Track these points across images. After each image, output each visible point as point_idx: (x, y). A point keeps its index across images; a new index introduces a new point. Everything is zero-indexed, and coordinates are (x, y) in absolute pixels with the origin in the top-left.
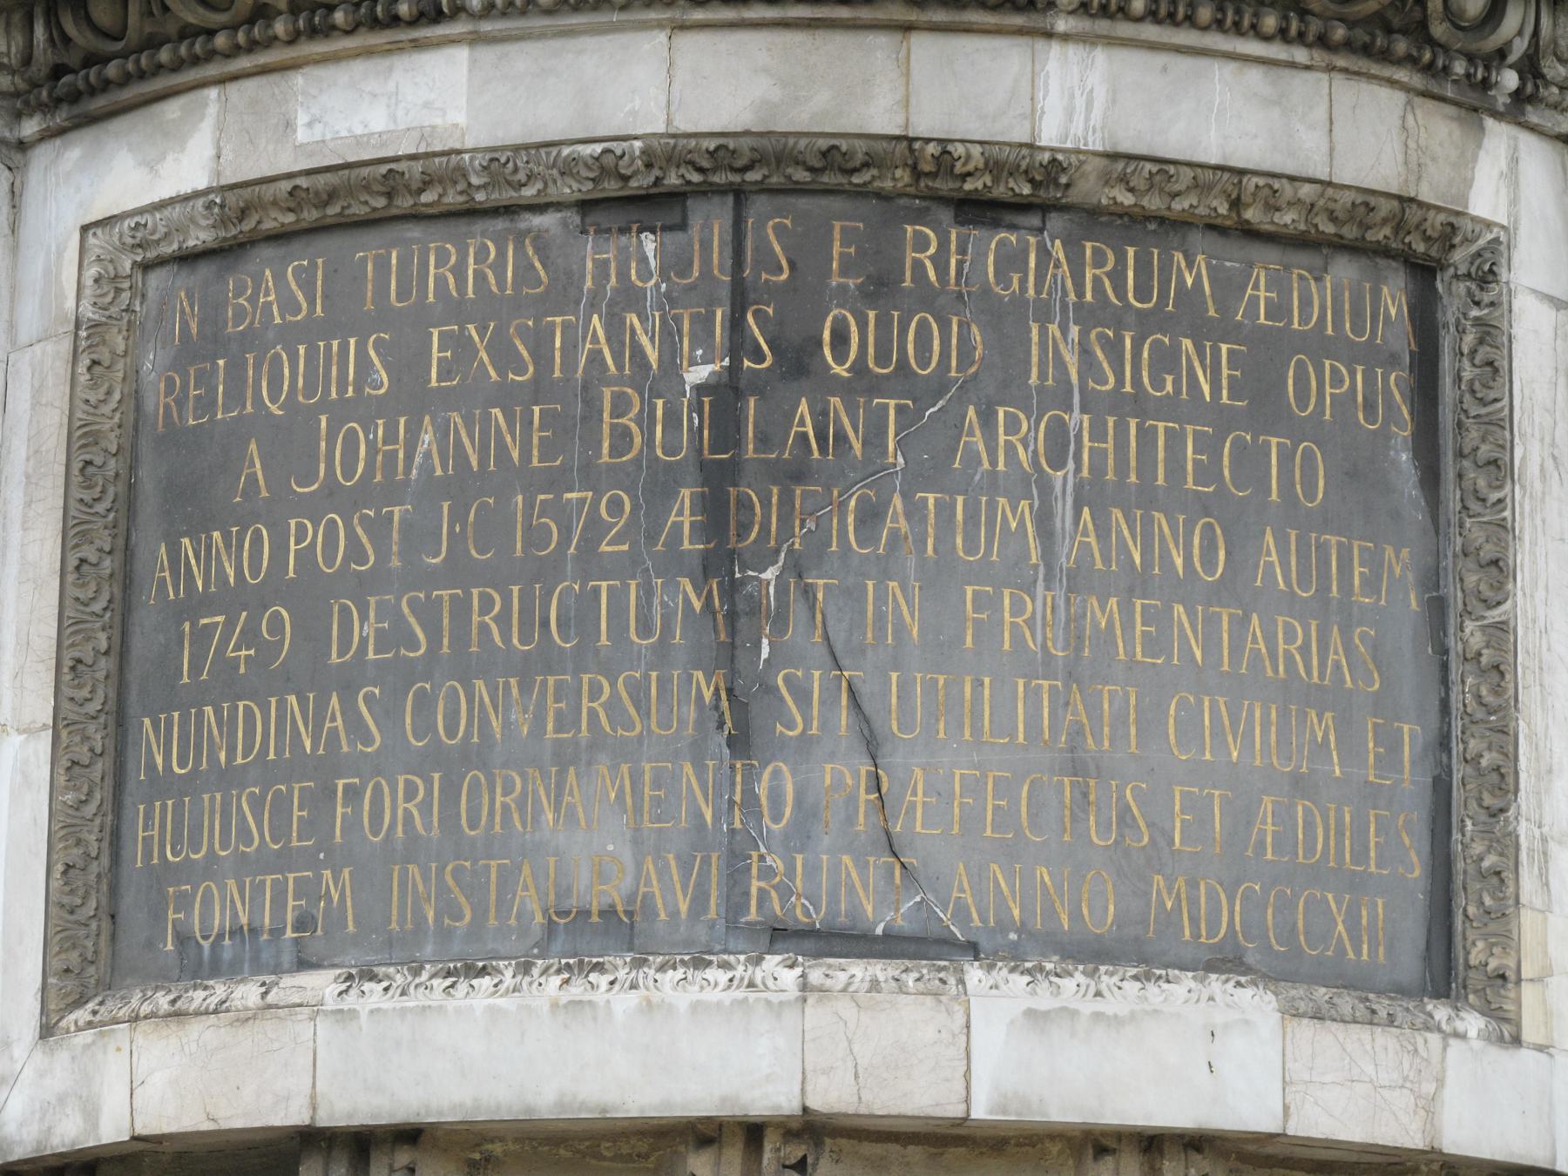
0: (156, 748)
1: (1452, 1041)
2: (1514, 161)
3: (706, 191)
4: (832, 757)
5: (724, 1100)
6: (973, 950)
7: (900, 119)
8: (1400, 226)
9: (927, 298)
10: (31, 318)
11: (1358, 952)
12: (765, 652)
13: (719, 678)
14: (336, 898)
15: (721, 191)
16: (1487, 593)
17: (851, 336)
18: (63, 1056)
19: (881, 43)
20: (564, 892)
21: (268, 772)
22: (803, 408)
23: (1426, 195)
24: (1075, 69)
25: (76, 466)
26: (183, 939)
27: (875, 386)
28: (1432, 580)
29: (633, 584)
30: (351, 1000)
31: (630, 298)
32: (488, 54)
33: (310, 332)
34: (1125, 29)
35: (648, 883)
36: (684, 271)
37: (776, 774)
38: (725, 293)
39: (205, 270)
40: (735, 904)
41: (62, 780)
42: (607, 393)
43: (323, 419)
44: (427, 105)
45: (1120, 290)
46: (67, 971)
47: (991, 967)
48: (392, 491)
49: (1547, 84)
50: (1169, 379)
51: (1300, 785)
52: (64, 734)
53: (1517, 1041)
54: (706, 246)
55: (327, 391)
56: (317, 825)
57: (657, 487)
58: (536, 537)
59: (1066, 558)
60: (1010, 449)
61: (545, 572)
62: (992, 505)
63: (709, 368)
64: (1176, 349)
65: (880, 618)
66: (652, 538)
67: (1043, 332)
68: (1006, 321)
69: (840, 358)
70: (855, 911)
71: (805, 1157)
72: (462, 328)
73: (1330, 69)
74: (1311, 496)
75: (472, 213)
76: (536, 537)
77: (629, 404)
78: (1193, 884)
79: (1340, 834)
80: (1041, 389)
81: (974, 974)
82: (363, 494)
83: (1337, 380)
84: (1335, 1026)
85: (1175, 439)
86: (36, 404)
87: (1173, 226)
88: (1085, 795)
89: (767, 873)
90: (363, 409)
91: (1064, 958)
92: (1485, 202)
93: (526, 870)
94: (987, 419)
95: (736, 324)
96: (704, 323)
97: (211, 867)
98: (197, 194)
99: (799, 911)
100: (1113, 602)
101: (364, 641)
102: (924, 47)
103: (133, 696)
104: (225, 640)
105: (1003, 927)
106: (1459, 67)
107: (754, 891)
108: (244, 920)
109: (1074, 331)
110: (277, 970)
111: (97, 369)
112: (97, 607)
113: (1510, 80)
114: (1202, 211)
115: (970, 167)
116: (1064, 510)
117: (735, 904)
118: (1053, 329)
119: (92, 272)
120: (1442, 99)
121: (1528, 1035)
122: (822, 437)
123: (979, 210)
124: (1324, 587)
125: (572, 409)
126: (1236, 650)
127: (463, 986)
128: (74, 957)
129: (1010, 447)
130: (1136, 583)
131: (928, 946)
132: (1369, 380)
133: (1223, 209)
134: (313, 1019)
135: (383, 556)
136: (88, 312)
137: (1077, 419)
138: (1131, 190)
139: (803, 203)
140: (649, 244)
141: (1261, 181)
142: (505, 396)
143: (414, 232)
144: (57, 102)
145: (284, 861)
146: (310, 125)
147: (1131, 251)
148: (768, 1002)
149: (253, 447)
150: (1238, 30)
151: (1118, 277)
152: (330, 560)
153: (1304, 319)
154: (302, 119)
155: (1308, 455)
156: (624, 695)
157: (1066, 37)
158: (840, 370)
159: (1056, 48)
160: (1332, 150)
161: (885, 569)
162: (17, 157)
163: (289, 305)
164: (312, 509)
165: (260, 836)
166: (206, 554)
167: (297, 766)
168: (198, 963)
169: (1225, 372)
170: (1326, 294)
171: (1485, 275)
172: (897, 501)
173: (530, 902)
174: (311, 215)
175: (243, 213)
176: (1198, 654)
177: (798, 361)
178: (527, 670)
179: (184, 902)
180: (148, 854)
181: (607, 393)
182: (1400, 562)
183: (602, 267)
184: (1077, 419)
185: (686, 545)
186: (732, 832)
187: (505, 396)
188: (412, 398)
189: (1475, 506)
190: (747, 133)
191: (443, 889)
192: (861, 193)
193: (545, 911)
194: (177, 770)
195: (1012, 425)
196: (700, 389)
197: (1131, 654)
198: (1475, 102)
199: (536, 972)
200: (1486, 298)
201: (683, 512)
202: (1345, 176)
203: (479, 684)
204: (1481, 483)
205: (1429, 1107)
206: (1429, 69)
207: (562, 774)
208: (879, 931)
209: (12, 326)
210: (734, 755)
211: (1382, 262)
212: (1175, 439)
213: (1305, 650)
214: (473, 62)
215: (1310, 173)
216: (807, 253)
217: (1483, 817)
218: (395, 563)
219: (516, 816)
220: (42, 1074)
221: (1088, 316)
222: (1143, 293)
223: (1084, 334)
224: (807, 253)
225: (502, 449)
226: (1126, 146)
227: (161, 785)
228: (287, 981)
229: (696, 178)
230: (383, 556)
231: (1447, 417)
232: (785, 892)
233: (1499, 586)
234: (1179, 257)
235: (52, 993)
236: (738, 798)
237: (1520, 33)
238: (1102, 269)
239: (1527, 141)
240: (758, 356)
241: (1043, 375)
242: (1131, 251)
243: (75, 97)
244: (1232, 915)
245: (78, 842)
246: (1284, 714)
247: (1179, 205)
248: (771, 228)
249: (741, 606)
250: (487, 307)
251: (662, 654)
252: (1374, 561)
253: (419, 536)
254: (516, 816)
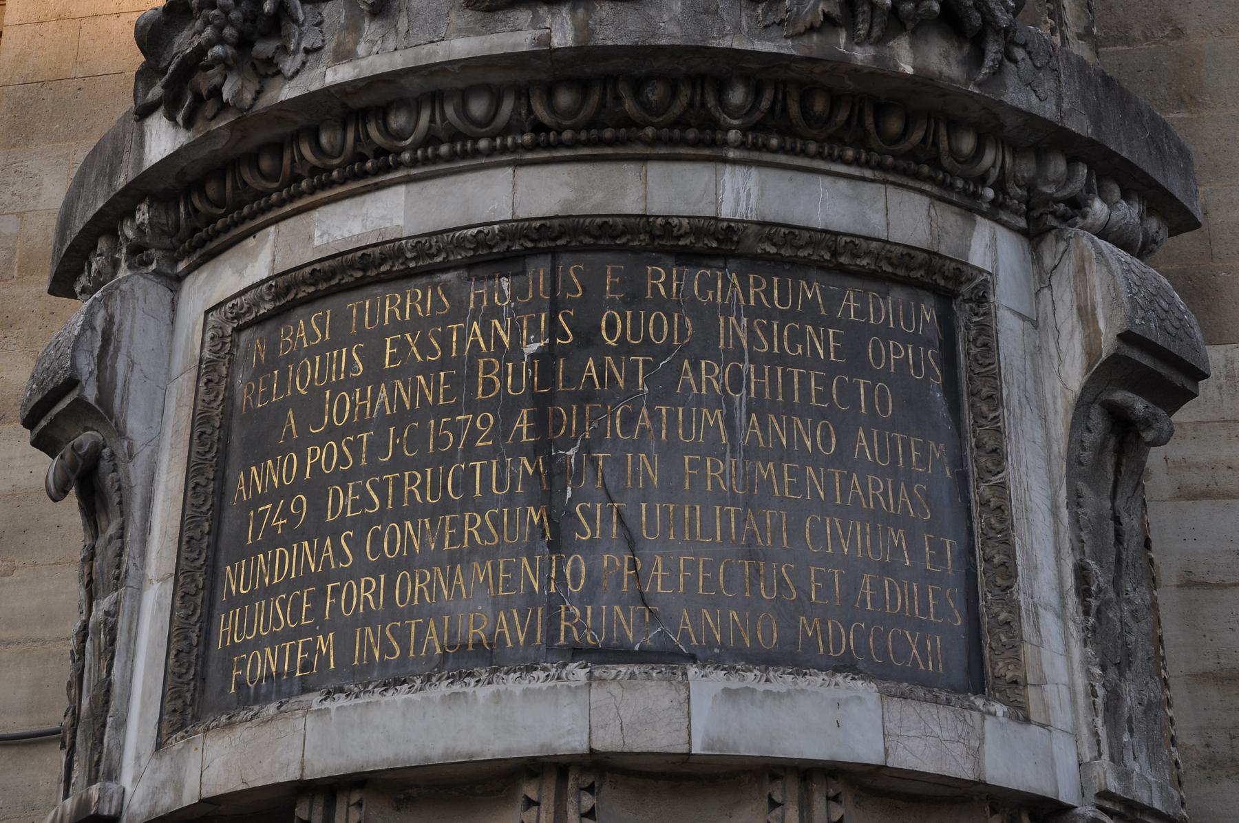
0: (234, 582)
1: (987, 717)
2: (994, 239)
3: (535, 252)
4: (608, 551)
5: (542, 746)
6: (693, 658)
7: (642, 206)
8: (930, 270)
9: (659, 303)
10: (178, 362)
11: (927, 666)
12: (569, 495)
13: (542, 510)
14: (324, 650)
15: (544, 252)
16: (992, 467)
17: (615, 326)
18: (167, 758)
19: (630, 169)
20: (453, 635)
21: (289, 585)
22: (591, 363)
23: (943, 251)
24: (740, 179)
25: (196, 435)
26: (241, 684)
27: (632, 350)
28: (958, 461)
29: (494, 462)
30: (327, 704)
31: (495, 312)
32: (415, 188)
33: (324, 348)
34: (768, 157)
35: (501, 626)
36: (524, 296)
37: (576, 561)
38: (546, 306)
39: (269, 326)
40: (551, 635)
41: (178, 603)
42: (481, 362)
43: (328, 393)
44: (383, 218)
45: (770, 299)
46: (175, 711)
47: (704, 667)
48: (363, 426)
49: (1011, 199)
50: (800, 347)
51: (885, 569)
52: (181, 578)
53: (1027, 720)
54: (536, 282)
55: (330, 378)
56: (314, 612)
57: (508, 409)
58: (441, 441)
59: (743, 440)
60: (709, 382)
61: (446, 460)
62: (699, 413)
63: (538, 345)
64: (803, 332)
65: (635, 474)
66: (505, 437)
67: (727, 322)
68: (705, 316)
69: (611, 337)
70: (623, 636)
71: (593, 783)
72: (403, 336)
73: (885, 182)
74: (885, 411)
75: (408, 275)
76: (441, 441)
77: (493, 367)
78: (824, 623)
79: (911, 598)
80: (726, 351)
81: (693, 670)
82: (350, 428)
83: (897, 352)
84: (913, 703)
85: (804, 379)
86: (178, 406)
87: (800, 266)
88: (758, 571)
89: (570, 617)
90: (350, 385)
91: (749, 661)
92: (978, 256)
93: (432, 625)
94: (695, 367)
95: (552, 321)
96: (534, 323)
97: (258, 643)
98: (263, 282)
99: (589, 638)
100: (771, 465)
101: (345, 507)
102: (655, 170)
103: (222, 556)
104: (271, 517)
105: (711, 644)
106: (960, 184)
107: (563, 627)
108: (274, 669)
109: (744, 321)
110: (290, 695)
111: (211, 384)
112: (204, 509)
113: (990, 193)
114: (815, 257)
115: (682, 231)
116: (740, 416)
117: (551, 635)
118: (732, 319)
119: (209, 334)
120: (950, 203)
121: (1034, 716)
122: (601, 378)
123: (689, 257)
124: (895, 461)
125: (462, 373)
126: (844, 492)
127: (391, 692)
128: (179, 703)
129: (709, 382)
130: (783, 455)
131: (667, 657)
132: (916, 353)
133: (827, 257)
134: (304, 716)
135: (357, 459)
136: (207, 355)
137: (747, 367)
138: (774, 245)
139: (590, 257)
140: (505, 283)
141: (848, 240)
142: (426, 369)
143: (378, 290)
144: (194, 249)
145: (298, 633)
146: (321, 236)
147: (776, 280)
148: (568, 687)
149: (290, 413)
150: (831, 158)
151: (769, 293)
152: (328, 467)
153: (877, 318)
154: (317, 233)
155: (882, 389)
156: (489, 523)
157: (734, 162)
158: (610, 342)
159: (729, 168)
160: (888, 224)
161: (637, 448)
162: (175, 285)
163: (311, 336)
164: (320, 441)
165: (285, 621)
166: (264, 475)
167: (306, 579)
168: (249, 698)
169: (832, 344)
170: (888, 306)
171: (981, 297)
172: (644, 411)
173: (433, 639)
174: (323, 286)
175: (288, 289)
176: (822, 494)
177: (588, 339)
178: (434, 513)
180: (224, 641)
181: (481, 362)
182: (938, 450)
183: (479, 298)
184: (747, 367)
185: (524, 439)
186: (550, 594)
187: (426, 369)
188: (375, 375)
189: (982, 421)
190: (556, 217)
191: (384, 639)
192: (623, 249)
193: (442, 647)
194: (242, 592)
195: (710, 370)
196: (532, 356)
197: (782, 491)
198: (970, 207)
199: (434, 679)
200: (982, 311)
201: (523, 423)
202: (896, 237)
203: (408, 523)
204: (985, 408)
205: (976, 755)
206: (941, 184)
207: (453, 570)
208: (637, 648)
209: (169, 370)
210: (551, 552)
211: (921, 292)
212: (804, 379)
213: (885, 494)
214: (408, 193)
215: (876, 235)
216: (592, 285)
217: (997, 591)
218: (364, 462)
219: (426, 594)
220: (154, 772)
221: (751, 313)
222: (783, 301)
223: (750, 323)
224: (592, 285)
225: (423, 395)
226: (770, 218)
227: (236, 601)
228: (294, 699)
229: (530, 245)
230: (357, 459)
231: (963, 375)
232: (581, 627)
233: (999, 464)
234: (803, 283)
235: (165, 724)
236: (553, 576)
237: (994, 166)
238: (760, 289)
239: (1001, 232)
240: (566, 337)
241: (727, 343)
242: (776, 280)
243: (202, 243)
244: (848, 641)
245: (186, 638)
246: (874, 529)
247: (802, 253)
248: (573, 270)
249: (555, 470)
250: (417, 323)
251: (510, 499)
252: (923, 448)
253: (377, 447)
254: (426, 594)
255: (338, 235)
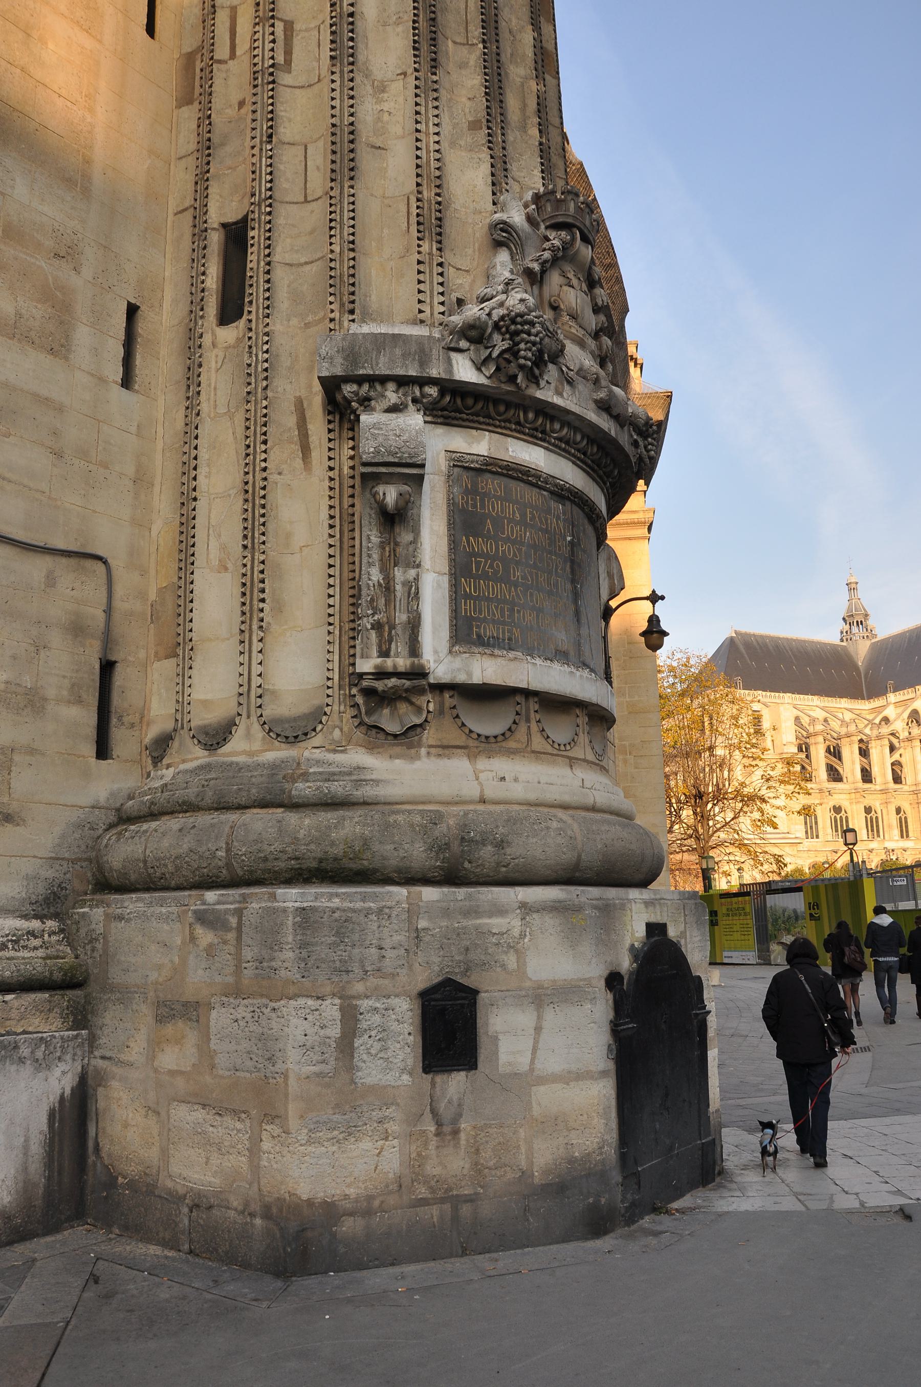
26: (479, 636)
145: (504, 623)
163: (495, 490)
175: (491, 464)
179: (478, 627)
187: (541, 529)
227: (468, 596)
255: (520, 455)
